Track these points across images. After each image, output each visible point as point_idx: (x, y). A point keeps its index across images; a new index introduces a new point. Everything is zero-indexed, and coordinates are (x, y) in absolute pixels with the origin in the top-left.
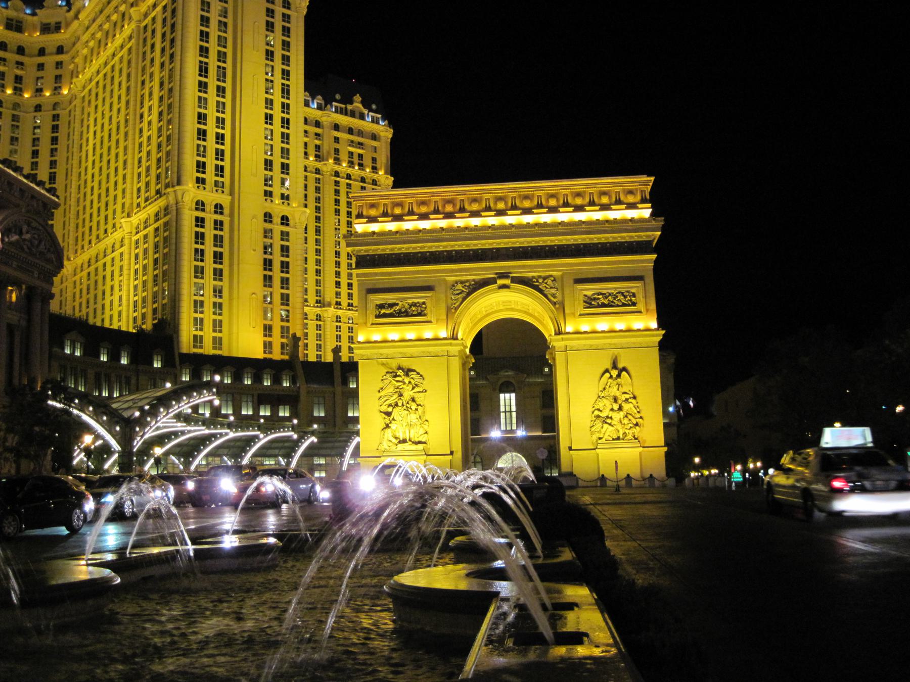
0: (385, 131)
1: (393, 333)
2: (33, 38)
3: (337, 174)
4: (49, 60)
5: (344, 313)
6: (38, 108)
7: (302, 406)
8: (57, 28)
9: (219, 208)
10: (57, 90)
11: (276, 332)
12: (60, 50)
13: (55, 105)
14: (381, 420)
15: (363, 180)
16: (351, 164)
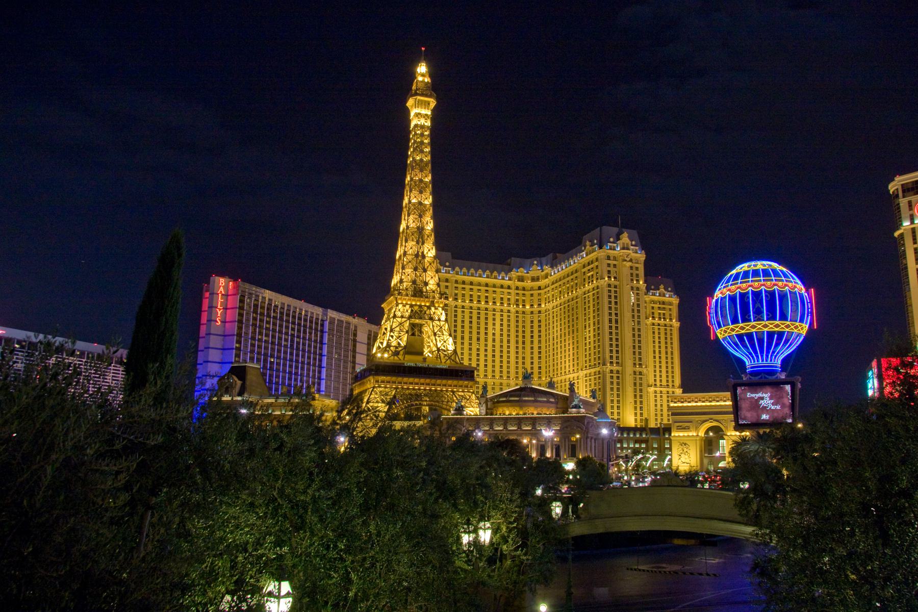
0: (675, 301)
1: (681, 434)
2: (528, 284)
3: (653, 324)
4: (536, 292)
5: (658, 389)
6: (532, 313)
7: (649, 443)
8: (538, 279)
9: (618, 372)
10: (540, 305)
11: (638, 415)
12: (540, 288)
13: (540, 312)
14: (678, 457)
15: (665, 325)
16: (660, 319)
